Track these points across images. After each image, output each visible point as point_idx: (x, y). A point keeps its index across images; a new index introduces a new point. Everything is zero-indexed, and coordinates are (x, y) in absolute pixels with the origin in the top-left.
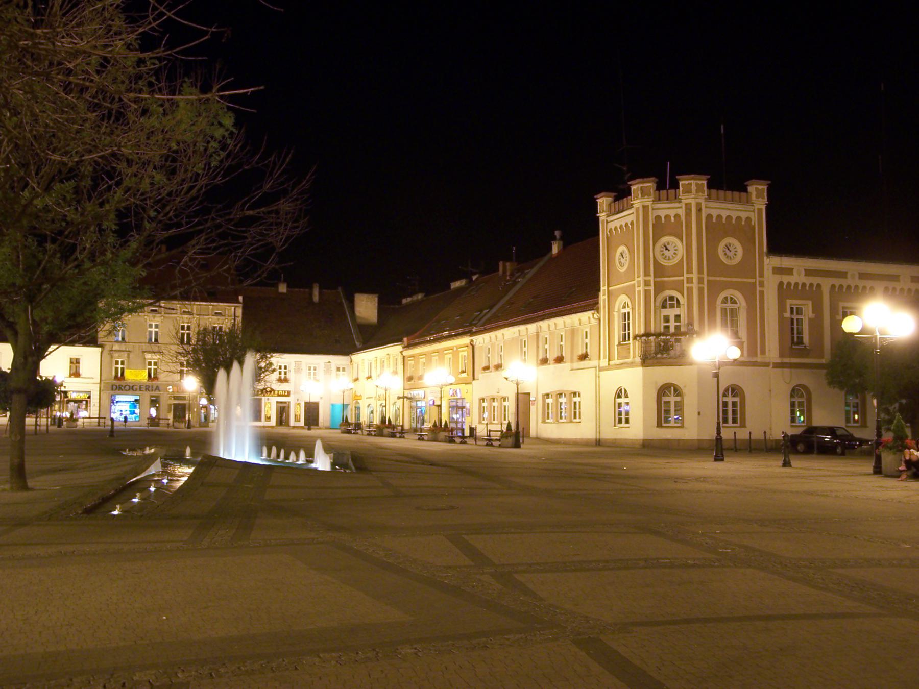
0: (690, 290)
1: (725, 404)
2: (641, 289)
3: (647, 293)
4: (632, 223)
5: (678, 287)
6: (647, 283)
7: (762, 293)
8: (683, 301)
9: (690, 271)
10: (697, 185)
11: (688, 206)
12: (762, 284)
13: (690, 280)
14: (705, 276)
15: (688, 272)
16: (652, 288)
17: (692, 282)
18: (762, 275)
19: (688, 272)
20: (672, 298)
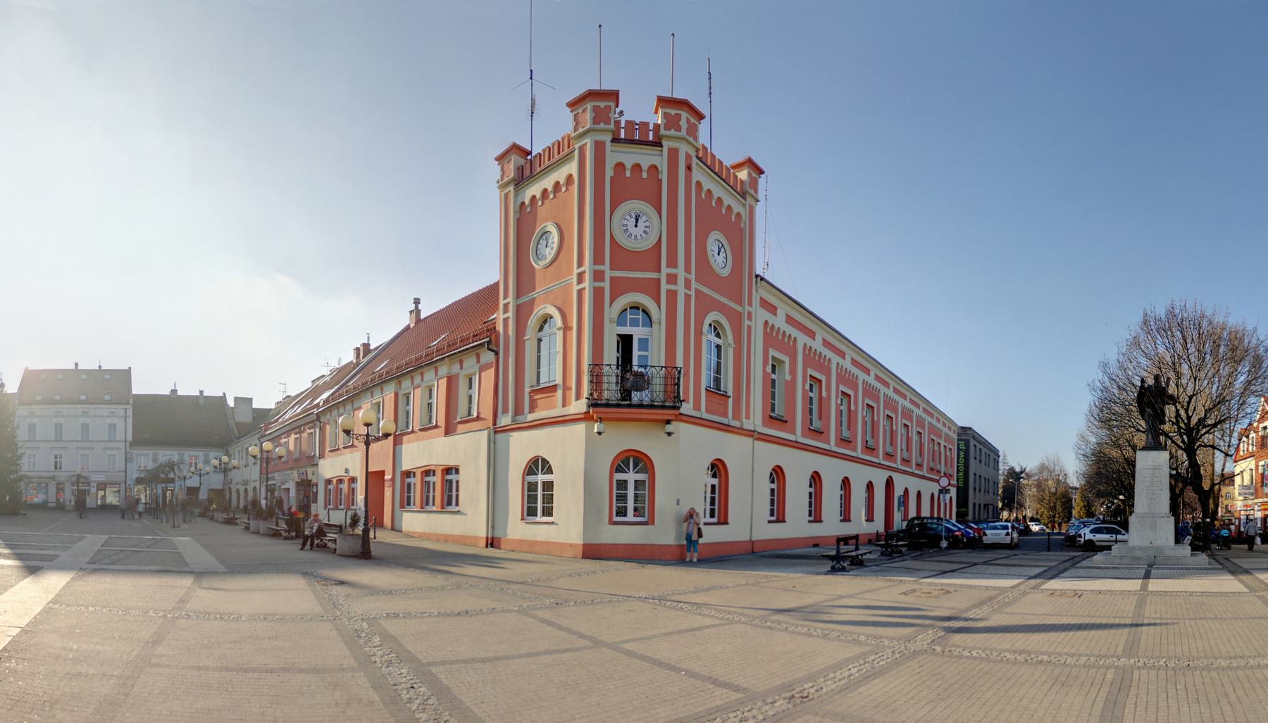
0: (672, 295)
1: (623, 485)
2: (586, 284)
3: (598, 294)
4: (570, 177)
5: (653, 289)
6: (598, 276)
7: (749, 327)
8: (659, 314)
9: (672, 263)
10: (688, 120)
11: (673, 153)
12: (750, 314)
13: (672, 279)
15: (668, 266)
16: (606, 285)
17: (675, 283)
18: (750, 304)
19: (668, 266)
20: (635, 307)
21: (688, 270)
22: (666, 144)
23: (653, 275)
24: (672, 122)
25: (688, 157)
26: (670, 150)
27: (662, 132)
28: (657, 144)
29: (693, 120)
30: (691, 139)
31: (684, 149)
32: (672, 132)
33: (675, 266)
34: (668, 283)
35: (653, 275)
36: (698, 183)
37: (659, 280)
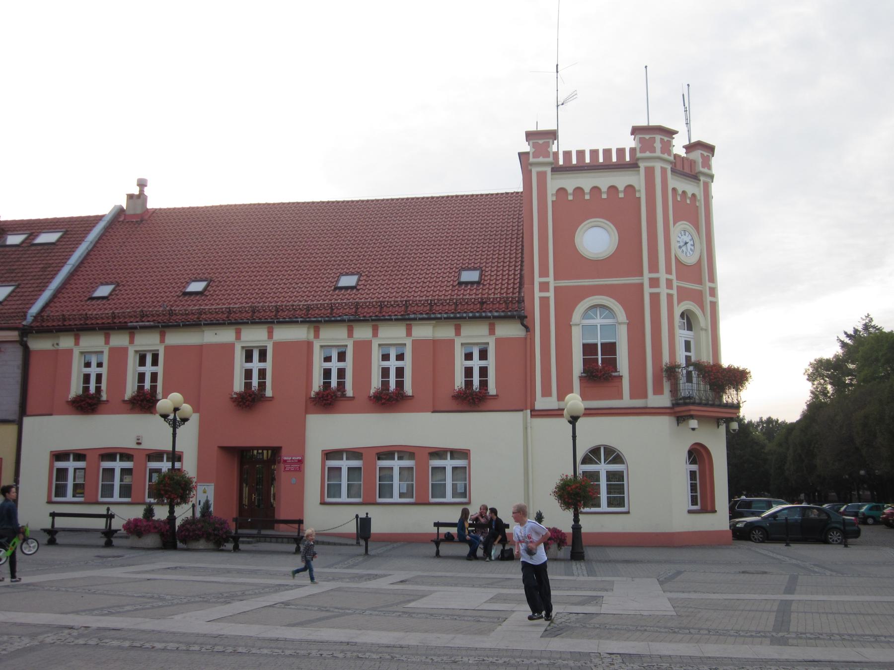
11: (650, 172)
14: (673, 277)
21: (669, 271)
22: (642, 165)
23: (634, 280)
24: (646, 145)
25: (664, 170)
26: (647, 168)
27: (639, 155)
28: (633, 165)
29: (666, 139)
30: (666, 156)
31: (658, 166)
32: (648, 154)
33: (657, 271)
34: (651, 286)
35: (634, 280)
36: (674, 190)
37: (642, 285)
